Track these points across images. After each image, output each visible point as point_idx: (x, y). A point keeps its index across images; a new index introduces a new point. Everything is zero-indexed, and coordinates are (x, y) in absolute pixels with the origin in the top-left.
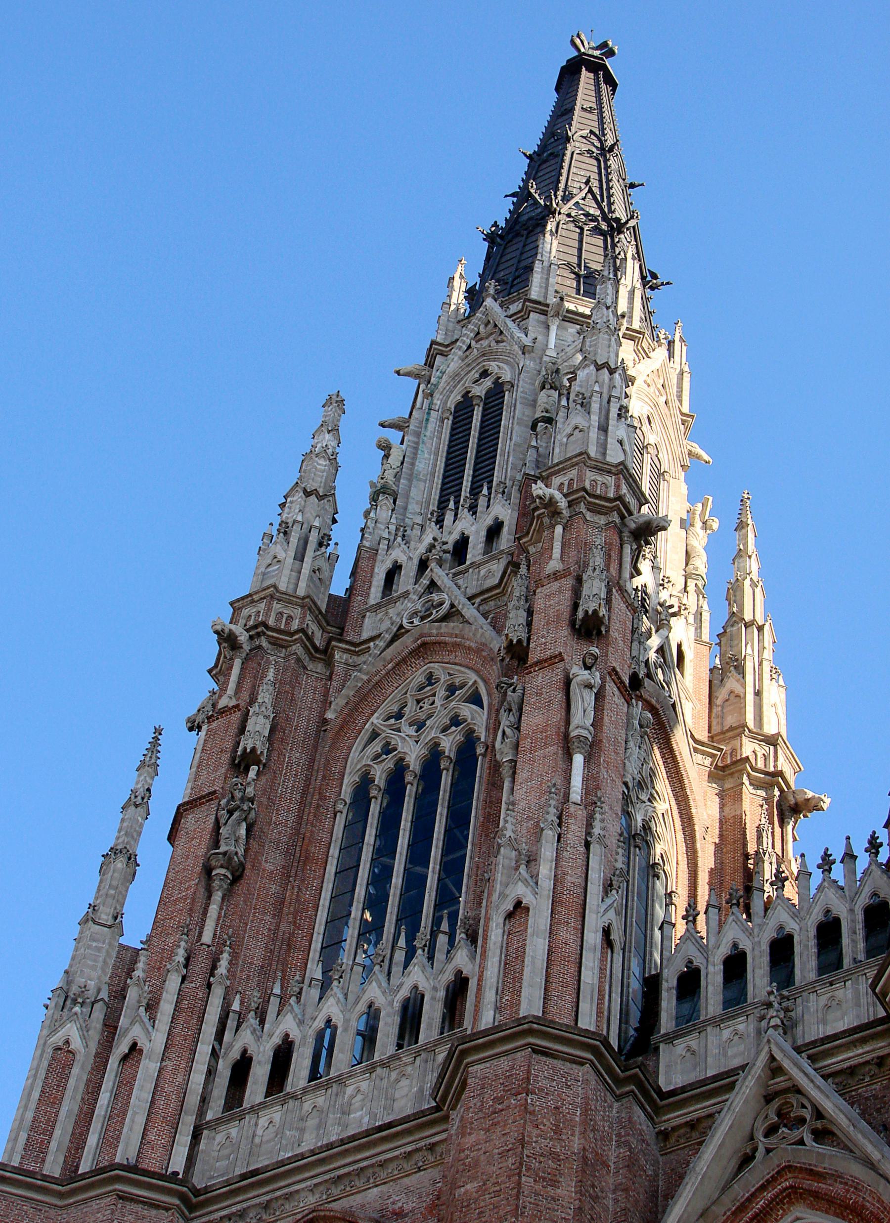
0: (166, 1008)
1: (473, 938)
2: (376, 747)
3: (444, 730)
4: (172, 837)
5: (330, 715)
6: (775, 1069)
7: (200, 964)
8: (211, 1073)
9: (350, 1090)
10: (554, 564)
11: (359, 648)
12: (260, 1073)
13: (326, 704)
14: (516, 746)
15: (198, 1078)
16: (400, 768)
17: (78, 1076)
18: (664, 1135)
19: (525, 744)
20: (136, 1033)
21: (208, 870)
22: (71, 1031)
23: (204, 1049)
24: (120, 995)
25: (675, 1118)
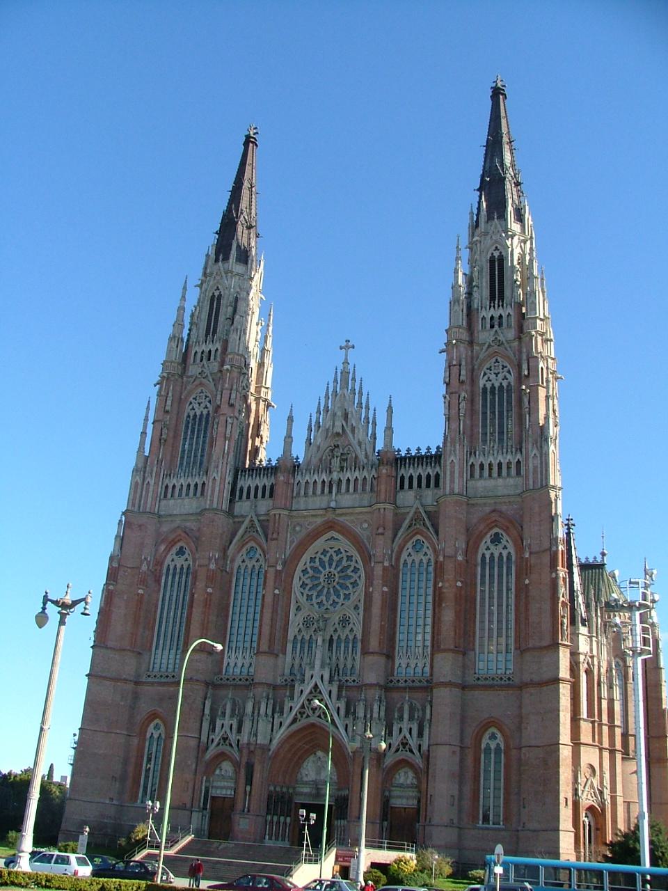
0: (154, 475)
3: (204, 408)
7: (160, 463)
8: (162, 487)
11: (188, 377)
12: (170, 490)
13: (181, 394)
15: (160, 490)
16: (195, 415)
18: (234, 522)
19: (218, 435)
21: (160, 440)
22: (138, 478)
23: (160, 483)
24: (145, 467)
25: (236, 520)
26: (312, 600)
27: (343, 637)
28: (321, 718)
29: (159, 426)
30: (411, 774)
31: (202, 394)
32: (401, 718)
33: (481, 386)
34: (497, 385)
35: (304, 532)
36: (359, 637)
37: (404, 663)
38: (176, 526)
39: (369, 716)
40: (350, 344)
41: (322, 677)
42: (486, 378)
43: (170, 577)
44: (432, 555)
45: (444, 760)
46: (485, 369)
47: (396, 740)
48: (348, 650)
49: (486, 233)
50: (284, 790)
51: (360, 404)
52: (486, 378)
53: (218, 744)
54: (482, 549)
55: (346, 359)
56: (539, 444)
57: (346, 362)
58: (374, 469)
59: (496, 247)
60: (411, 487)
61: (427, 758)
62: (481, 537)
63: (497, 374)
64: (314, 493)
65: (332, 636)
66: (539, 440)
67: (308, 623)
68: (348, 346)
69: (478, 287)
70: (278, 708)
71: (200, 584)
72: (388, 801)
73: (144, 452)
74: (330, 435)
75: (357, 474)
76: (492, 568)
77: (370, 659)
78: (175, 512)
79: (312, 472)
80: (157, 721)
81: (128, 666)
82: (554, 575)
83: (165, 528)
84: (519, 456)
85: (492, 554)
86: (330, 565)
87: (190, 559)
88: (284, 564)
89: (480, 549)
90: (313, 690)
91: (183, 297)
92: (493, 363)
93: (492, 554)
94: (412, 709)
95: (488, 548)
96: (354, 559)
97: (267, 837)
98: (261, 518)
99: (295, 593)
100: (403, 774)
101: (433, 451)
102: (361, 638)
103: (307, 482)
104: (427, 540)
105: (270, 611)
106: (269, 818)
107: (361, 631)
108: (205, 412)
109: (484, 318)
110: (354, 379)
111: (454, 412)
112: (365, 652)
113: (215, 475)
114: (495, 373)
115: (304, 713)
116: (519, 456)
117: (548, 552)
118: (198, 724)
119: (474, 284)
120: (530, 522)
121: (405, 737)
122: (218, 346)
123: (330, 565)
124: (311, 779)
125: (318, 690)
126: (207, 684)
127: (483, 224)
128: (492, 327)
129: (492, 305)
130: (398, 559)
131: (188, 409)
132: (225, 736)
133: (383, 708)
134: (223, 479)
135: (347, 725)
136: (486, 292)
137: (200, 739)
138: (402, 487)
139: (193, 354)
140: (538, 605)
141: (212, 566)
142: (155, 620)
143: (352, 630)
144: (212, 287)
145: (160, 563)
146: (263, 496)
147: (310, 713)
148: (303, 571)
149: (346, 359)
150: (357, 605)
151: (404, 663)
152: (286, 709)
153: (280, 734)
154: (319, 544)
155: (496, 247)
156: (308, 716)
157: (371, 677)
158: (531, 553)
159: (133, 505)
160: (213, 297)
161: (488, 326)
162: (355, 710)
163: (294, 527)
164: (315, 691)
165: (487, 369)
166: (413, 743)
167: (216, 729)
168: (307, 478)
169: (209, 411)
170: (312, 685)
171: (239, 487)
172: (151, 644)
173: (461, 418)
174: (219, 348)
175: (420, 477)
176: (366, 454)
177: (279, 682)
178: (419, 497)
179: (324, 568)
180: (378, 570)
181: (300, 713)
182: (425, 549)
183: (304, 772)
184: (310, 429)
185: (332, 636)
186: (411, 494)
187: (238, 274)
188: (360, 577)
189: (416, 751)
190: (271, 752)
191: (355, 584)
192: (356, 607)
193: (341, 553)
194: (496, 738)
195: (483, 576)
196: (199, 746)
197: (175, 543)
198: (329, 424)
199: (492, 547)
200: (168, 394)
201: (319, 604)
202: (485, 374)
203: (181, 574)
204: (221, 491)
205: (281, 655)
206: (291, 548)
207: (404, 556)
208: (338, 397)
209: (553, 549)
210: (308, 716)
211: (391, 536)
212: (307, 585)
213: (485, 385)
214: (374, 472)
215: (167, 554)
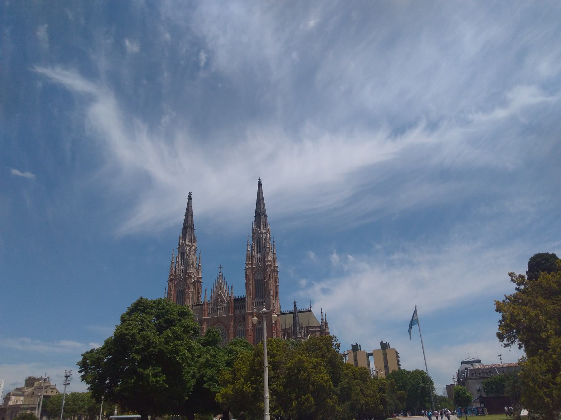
40: (221, 267)
60: (238, 309)
63: (259, 275)
76: (259, 331)
84: (264, 300)
85: (259, 327)
95: (258, 325)
108: (182, 290)
116: (264, 300)
130: (236, 330)
138: (236, 309)
149: (220, 271)
182: (243, 326)
186: (239, 310)
188: (226, 335)
199: (259, 325)
207: (237, 329)
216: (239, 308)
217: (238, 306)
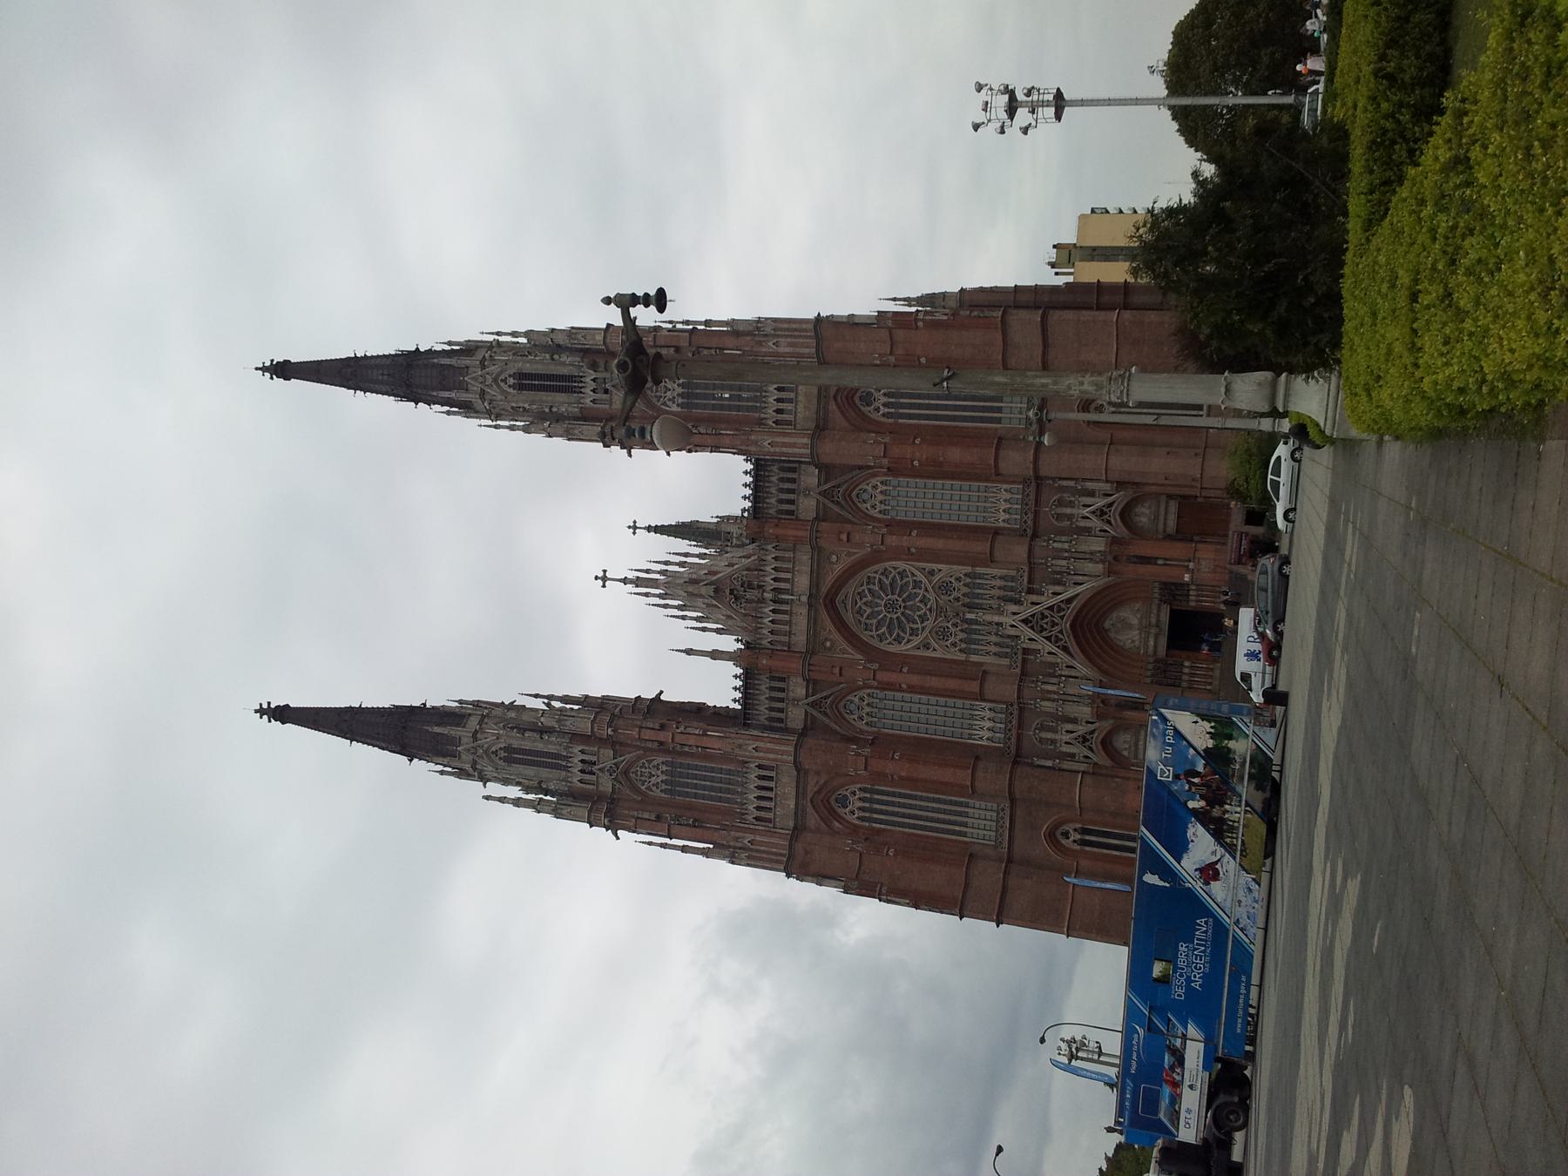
1: (746, 762)
2: (654, 788)
3: (658, 769)
4: (671, 839)
5: (640, 798)
6: (808, 704)
9: (779, 792)
10: (635, 733)
12: (762, 814)
14: (697, 747)
15: (760, 828)
17: (754, 854)
18: (811, 729)
20: (746, 842)
21: (695, 826)
22: (743, 855)
24: (730, 847)
26: (917, 629)
27: (966, 590)
28: (1064, 615)
29: (674, 831)
30: (1139, 509)
31: (639, 773)
32: (1070, 517)
33: (679, 409)
34: (680, 390)
35: (836, 636)
36: (969, 569)
37: (1003, 516)
38: (809, 804)
39: (1066, 554)
41: (1014, 614)
42: (669, 403)
43: (875, 816)
44: (879, 478)
45: (1125, 463)
46: (659, 404)
47: (1096, 523)
48: (982, 594)
49: (482, 394)
50: (1150, 667)
51: (681, 564)
52: (669, 403)
53: (1091, 749)
54: (875, 416)
55: (620, 580)
56: (762, 339)
57: (625, 581)
58: (765, 547)
59: (502, 381)
60: (792, 502)
61: (1120, 485)
62: (864, 416)
64: (785, 623)
65: (964, 605)
66: (757, 339)
67: (942, 634)
68: (604, 579)
69: (551, 407)
70: (1051, 670)
71: (890, 768)
72: (1169, 535)
73: (709, 848)
74: (716, 603)
75: (768, 569)
76: (903, 406)
77: (998, 555)
78: (792, 806)
79: (759, 625)
80: (1059, 836)
81: (988, 877)
82: (920, 324)
83: (813, 819)
85: (885, 405)
86: (878, 605)
87: (853, 788)
88: (871, 662)
89: (876, 418)
90: (1030, 625)
91: (502, 800)
92: (653, 394)
93: (885, 405)
94: (1060, 503)
95: (877, 410)
96: (872, 575)
97: (1208, 687)
98: (810, 691)
99: (907, 650)
100: (1138, 519)
101: (749, 466)
102: (970, 568)
103: (771, 632)
104: (858, 485)
105: (929, 677)
106: (1184, 684)
107: (961, 567)
109: (594, 401)
110: (647, 571)
111: (710, 440)
112: (991, 560)
113: (750, 748)
114: (665, 392)
115: (1056, 636)
117: (894, 331)
118: (1065, 773)
119: (547, 410)
120: (853, 353)
121: (1094, 512)
122: (577, 749)
123: (878, 605)
124: (1138, 637)
125: (1030, 618)
126: (1015, 763)
127: (468, 395)
128: (606, 391)
129: (578, 390)
130: (878, 520)
131: (657, 793)
132: (1081, 740)
133: (1057, 538)
134: (757, 738)
135: (1075, 584)
136: (561, 397)
137: (1083, 772)
138: (791, 513)
139: (582, 785)
140: (953, 347)
141: (867, 751)
142: (927, 837)
143: (958, 579)
144: (492, 761)
145: (854, 830)
146: (782, 690)
147: (1057, 628)
148: (881, 641)
149: (620, 580)
150: (929, 573)
151: (1003, 516)
152: (1051, 659)
153: (1083, 669)
154: (849, 617)
155: (502, 381)
156: (1061, 632)
157: (1020, 551)
158: (891, 354)
159: (777, 862)
160: (505, 759)
161: (605, 396)
162: (1058, 573)
163: (825, 648)
164: (1031, 622)
165: (658, 401)
166: (1100, 502)
167: (1071, 751)
168: (765, 631)
169: (663, 763)
170: (1023, 627)
171: (766, 723)
172: (960, 842)
173: (718, 432)
174: (580, 748)
175: (781, 490)
176: (744, 557)
177: (1018, 671)
178: (807, 492)
179: (879, 613)
180: (892, 540)
181: (1056, 642)
182: (869, 488)
183: (1128, 644)
184: (704, 629)
185: (964, 605)
187: (480, 723)
188: (895, 568)
189: (1110, 499)
190: (1104, 680)
191: (902, 574)
192: (932, 573)
193: (863, 591)
194: (1102, 405)
195: (910, 416)
196: (1093, 773)
197: (833, 810)
198: (699, 602)
199: (876, 404)
200: (633, 817)
201: (923, 618)
202: (665, 404)
203: (871, 801)
204: (773, 740)
205: (984, 668)
206: (853, 652)
207: (873, 512)
208: (668, 592)
209: (890, 325)
210: (1061, 632)
211: (850, 526)
212: (898, 635)
213: (678, 405)
214: (770, 547)
215: (843, 819)
216: (791, 496)
217: (781, 501)
